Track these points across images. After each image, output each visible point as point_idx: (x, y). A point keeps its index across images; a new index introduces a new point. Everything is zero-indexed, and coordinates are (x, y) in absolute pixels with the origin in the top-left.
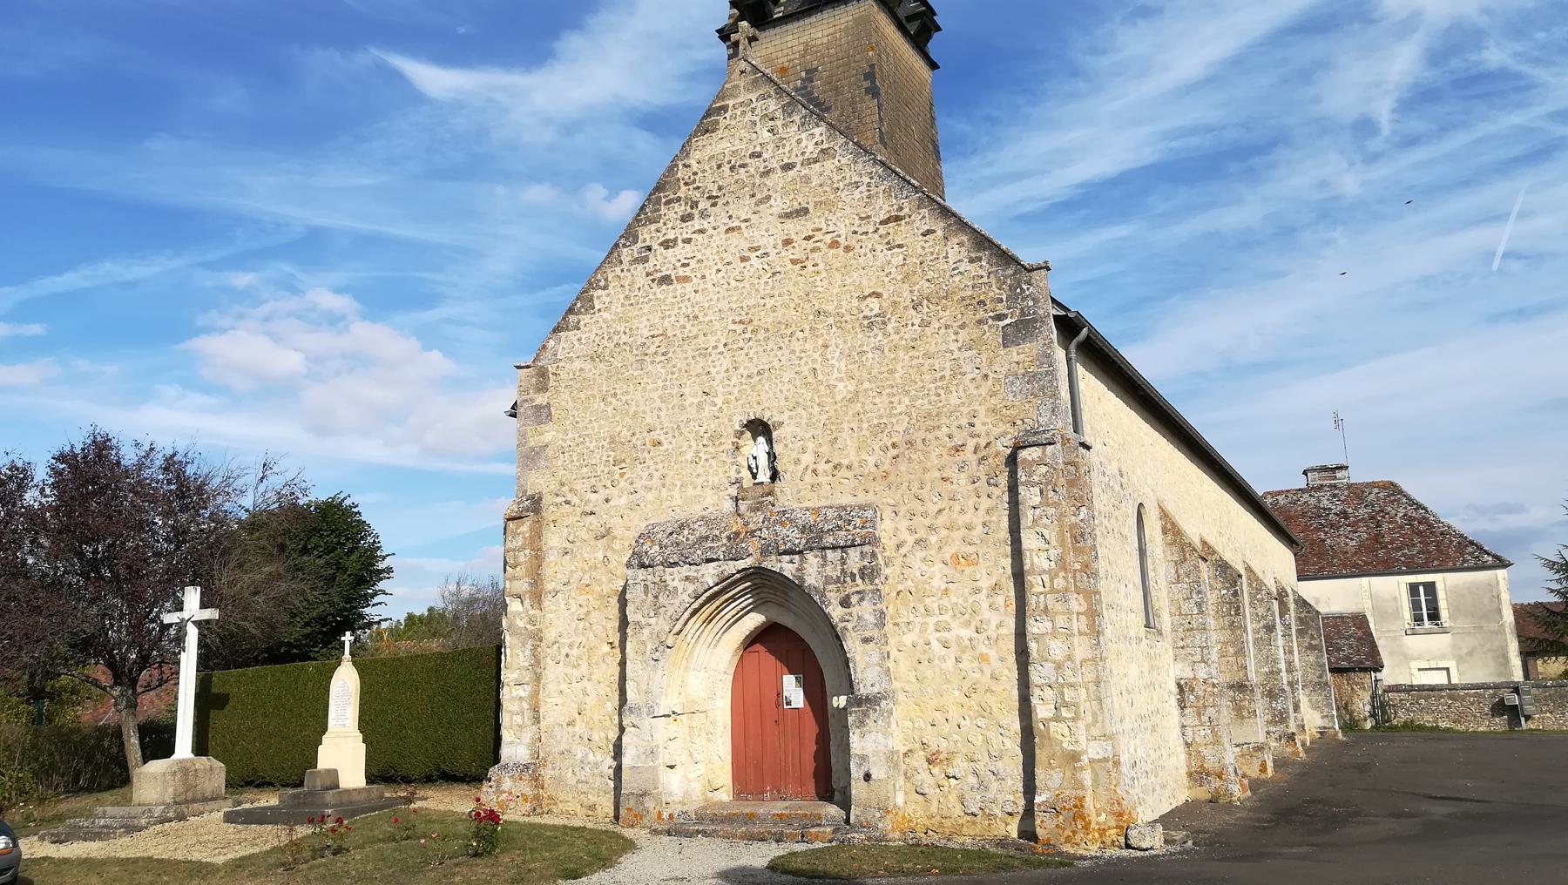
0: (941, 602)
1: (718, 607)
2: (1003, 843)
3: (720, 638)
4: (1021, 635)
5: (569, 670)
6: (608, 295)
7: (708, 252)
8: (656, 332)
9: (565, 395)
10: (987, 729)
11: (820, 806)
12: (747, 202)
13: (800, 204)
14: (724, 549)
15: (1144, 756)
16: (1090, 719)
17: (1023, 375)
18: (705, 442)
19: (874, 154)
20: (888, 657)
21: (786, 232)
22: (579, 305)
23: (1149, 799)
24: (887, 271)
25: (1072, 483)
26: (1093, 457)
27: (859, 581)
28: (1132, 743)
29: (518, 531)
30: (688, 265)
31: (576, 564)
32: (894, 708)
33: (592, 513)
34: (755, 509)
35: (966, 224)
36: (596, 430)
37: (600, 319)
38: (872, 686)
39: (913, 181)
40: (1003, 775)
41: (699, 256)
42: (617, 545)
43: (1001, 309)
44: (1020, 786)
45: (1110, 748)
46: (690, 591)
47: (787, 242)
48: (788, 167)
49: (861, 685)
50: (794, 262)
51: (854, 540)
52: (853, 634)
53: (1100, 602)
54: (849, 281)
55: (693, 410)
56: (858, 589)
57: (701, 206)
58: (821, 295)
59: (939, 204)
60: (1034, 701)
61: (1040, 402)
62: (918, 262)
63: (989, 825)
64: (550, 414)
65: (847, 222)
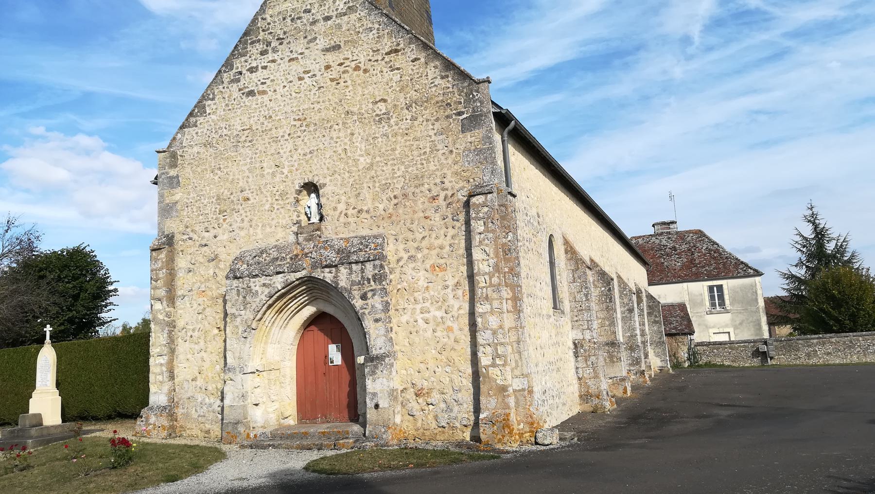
0: (424, 295)
1: (285, 303)
2: (459, 444)
3: (288, 322)
4: (472, 314)
5: (193, 346)
6: (215, 104)
7: (278, 74)
8: (245, 127)
9: (188, 169)
10: (452, 373)
11: (349, 426)
12: (302, 42)
13: (335, 42)
14: (288, 265)
15: (552, 387)
16: (513, 365)
17: (474, 150)
18: (277, 198)
19: (381, 9)
20: (391, 331)
21: (327, 61)
22: (196, 111)
23: (554, 413)
24: (390, 85)
25: (503, 218)
26: (518, 203)
27: (372, 283)
28: (544, 379)
29: (159, 258)
30: (265, 83)
31: (196, 278)
32: (395, 362)
33: (206, 245)
34: (308, 240)
35: (439, 54)
36: (208, 192)
37: (210, 120)
38: (380, 349)
39: (406, 27)
40: (461, 401)
41: (272, 77)
42: (222, 265)
43: (461, 108)
44: (471, 408)
45: (526, 383)
46: (266, 293)
47: (328, 67)
48: (327, 18)
49: (373, 349)
50: (332, 80)
51: (369, 257)
52: (369, 317)
53: (520, 292)
54: (366, 92)
55: (269, 177)
56: (371, 288)
57: (273, 45)
58: (349, 101)
59: (422, 41)
60: (480, 354)
61: (484, 167)
62: (409, 79)
63: (453, 433)
64: (179, 182)
65: (365, 53)
